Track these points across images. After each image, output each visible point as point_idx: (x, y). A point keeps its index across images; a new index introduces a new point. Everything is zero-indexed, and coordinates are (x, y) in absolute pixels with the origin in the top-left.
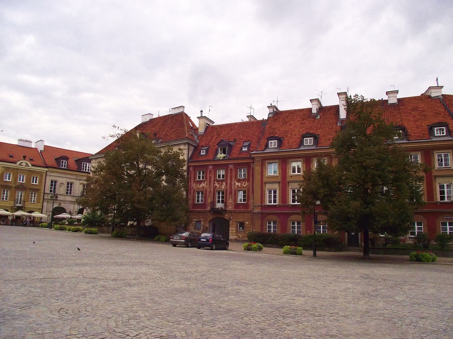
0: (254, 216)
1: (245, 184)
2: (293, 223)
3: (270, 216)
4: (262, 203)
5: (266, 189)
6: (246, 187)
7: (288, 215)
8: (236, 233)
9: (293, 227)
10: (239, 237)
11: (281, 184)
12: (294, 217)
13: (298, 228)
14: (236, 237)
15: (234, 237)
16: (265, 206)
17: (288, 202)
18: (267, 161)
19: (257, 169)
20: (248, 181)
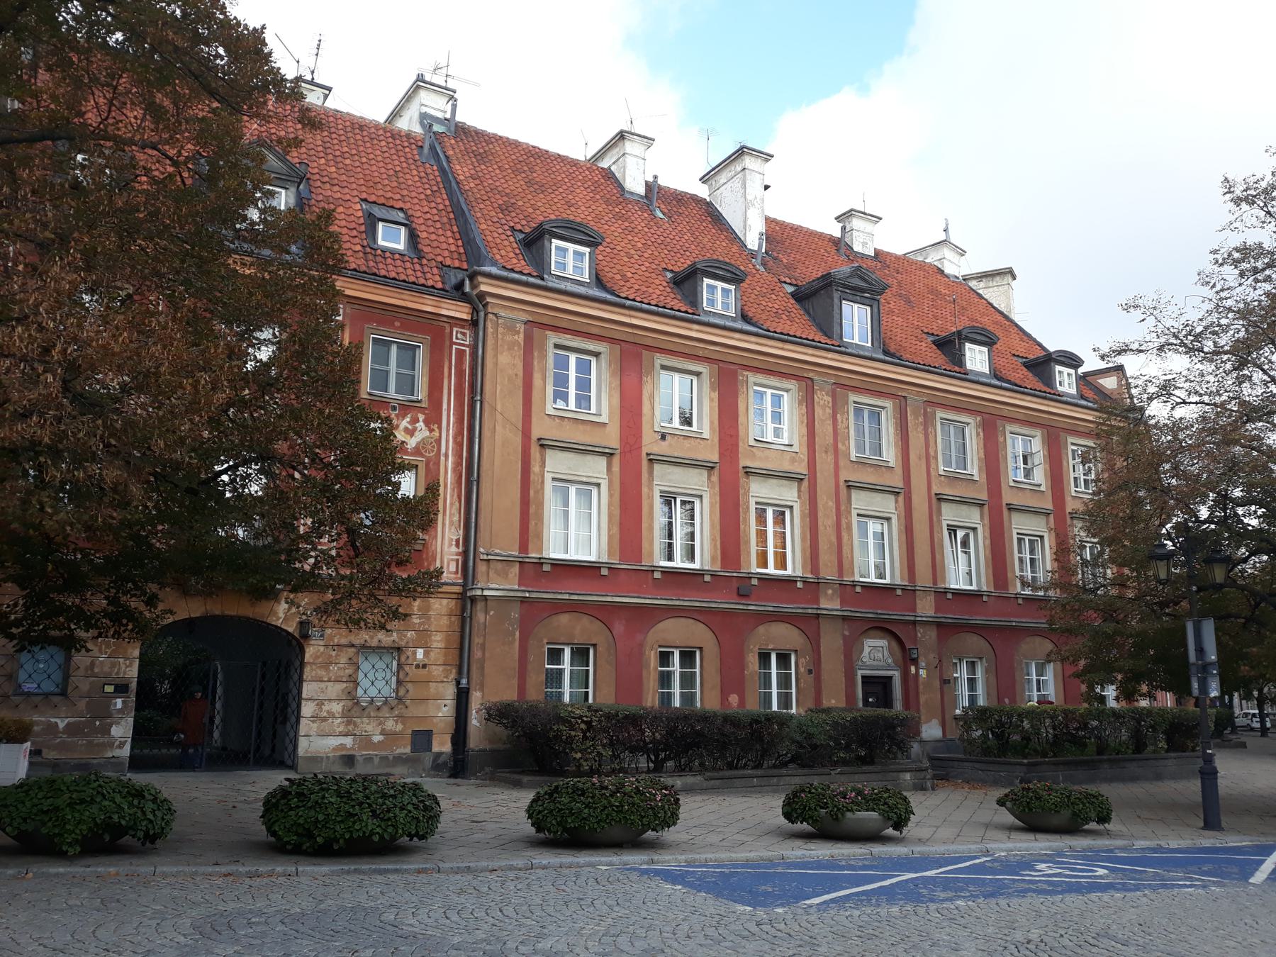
0: (480, 617)
1: (411, 433)
2: (665, 658)
3: (564, 619)
4: (524, 547)
5: (548, 477)
6: (417, 451)
7: (645, 616)
8: (348, 716)
9: (665, 679)
10: (366, 741)
11: (616, 460)
12: (675, 631)
13: (687, 680)
14: (348, 741)
15: (333, 742)
16: (540, 563)
17: (651, 554)
18: (553, 338)
19: (503, 362)
20: (433, 419)
